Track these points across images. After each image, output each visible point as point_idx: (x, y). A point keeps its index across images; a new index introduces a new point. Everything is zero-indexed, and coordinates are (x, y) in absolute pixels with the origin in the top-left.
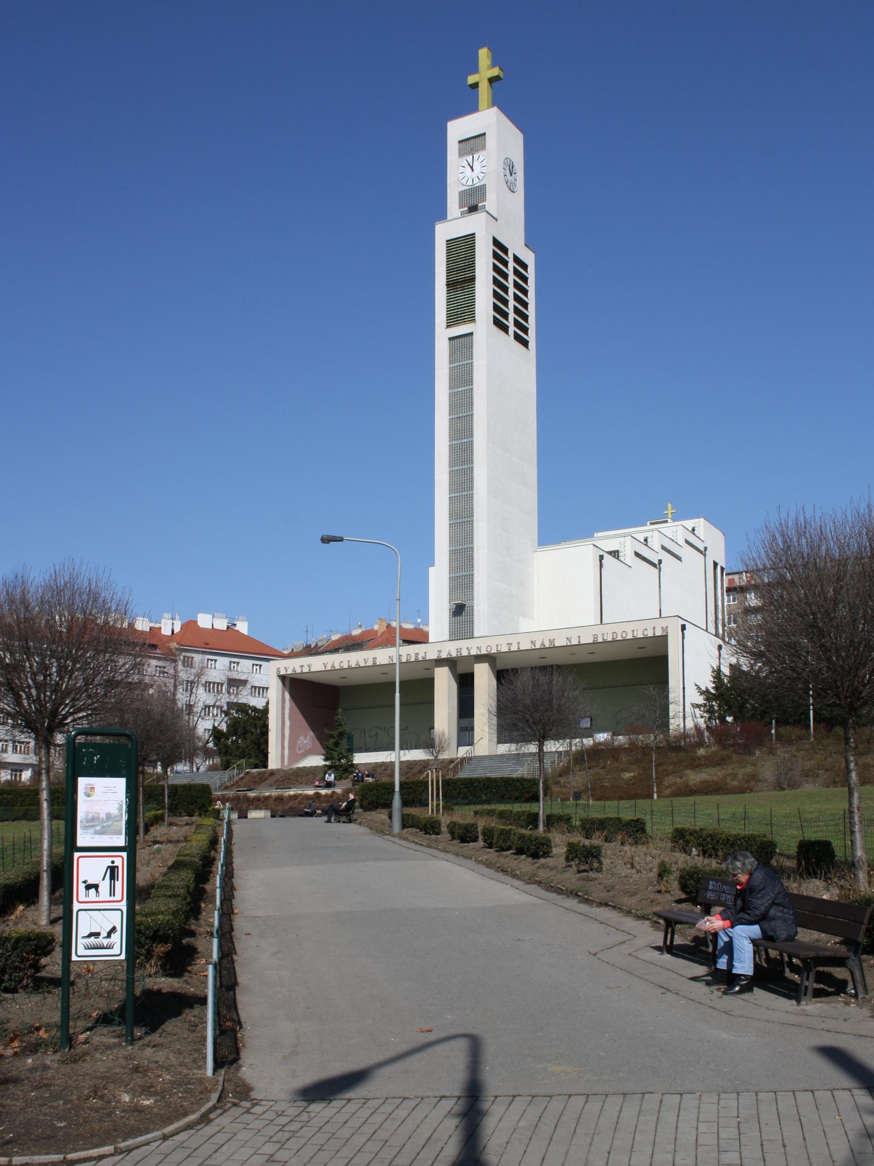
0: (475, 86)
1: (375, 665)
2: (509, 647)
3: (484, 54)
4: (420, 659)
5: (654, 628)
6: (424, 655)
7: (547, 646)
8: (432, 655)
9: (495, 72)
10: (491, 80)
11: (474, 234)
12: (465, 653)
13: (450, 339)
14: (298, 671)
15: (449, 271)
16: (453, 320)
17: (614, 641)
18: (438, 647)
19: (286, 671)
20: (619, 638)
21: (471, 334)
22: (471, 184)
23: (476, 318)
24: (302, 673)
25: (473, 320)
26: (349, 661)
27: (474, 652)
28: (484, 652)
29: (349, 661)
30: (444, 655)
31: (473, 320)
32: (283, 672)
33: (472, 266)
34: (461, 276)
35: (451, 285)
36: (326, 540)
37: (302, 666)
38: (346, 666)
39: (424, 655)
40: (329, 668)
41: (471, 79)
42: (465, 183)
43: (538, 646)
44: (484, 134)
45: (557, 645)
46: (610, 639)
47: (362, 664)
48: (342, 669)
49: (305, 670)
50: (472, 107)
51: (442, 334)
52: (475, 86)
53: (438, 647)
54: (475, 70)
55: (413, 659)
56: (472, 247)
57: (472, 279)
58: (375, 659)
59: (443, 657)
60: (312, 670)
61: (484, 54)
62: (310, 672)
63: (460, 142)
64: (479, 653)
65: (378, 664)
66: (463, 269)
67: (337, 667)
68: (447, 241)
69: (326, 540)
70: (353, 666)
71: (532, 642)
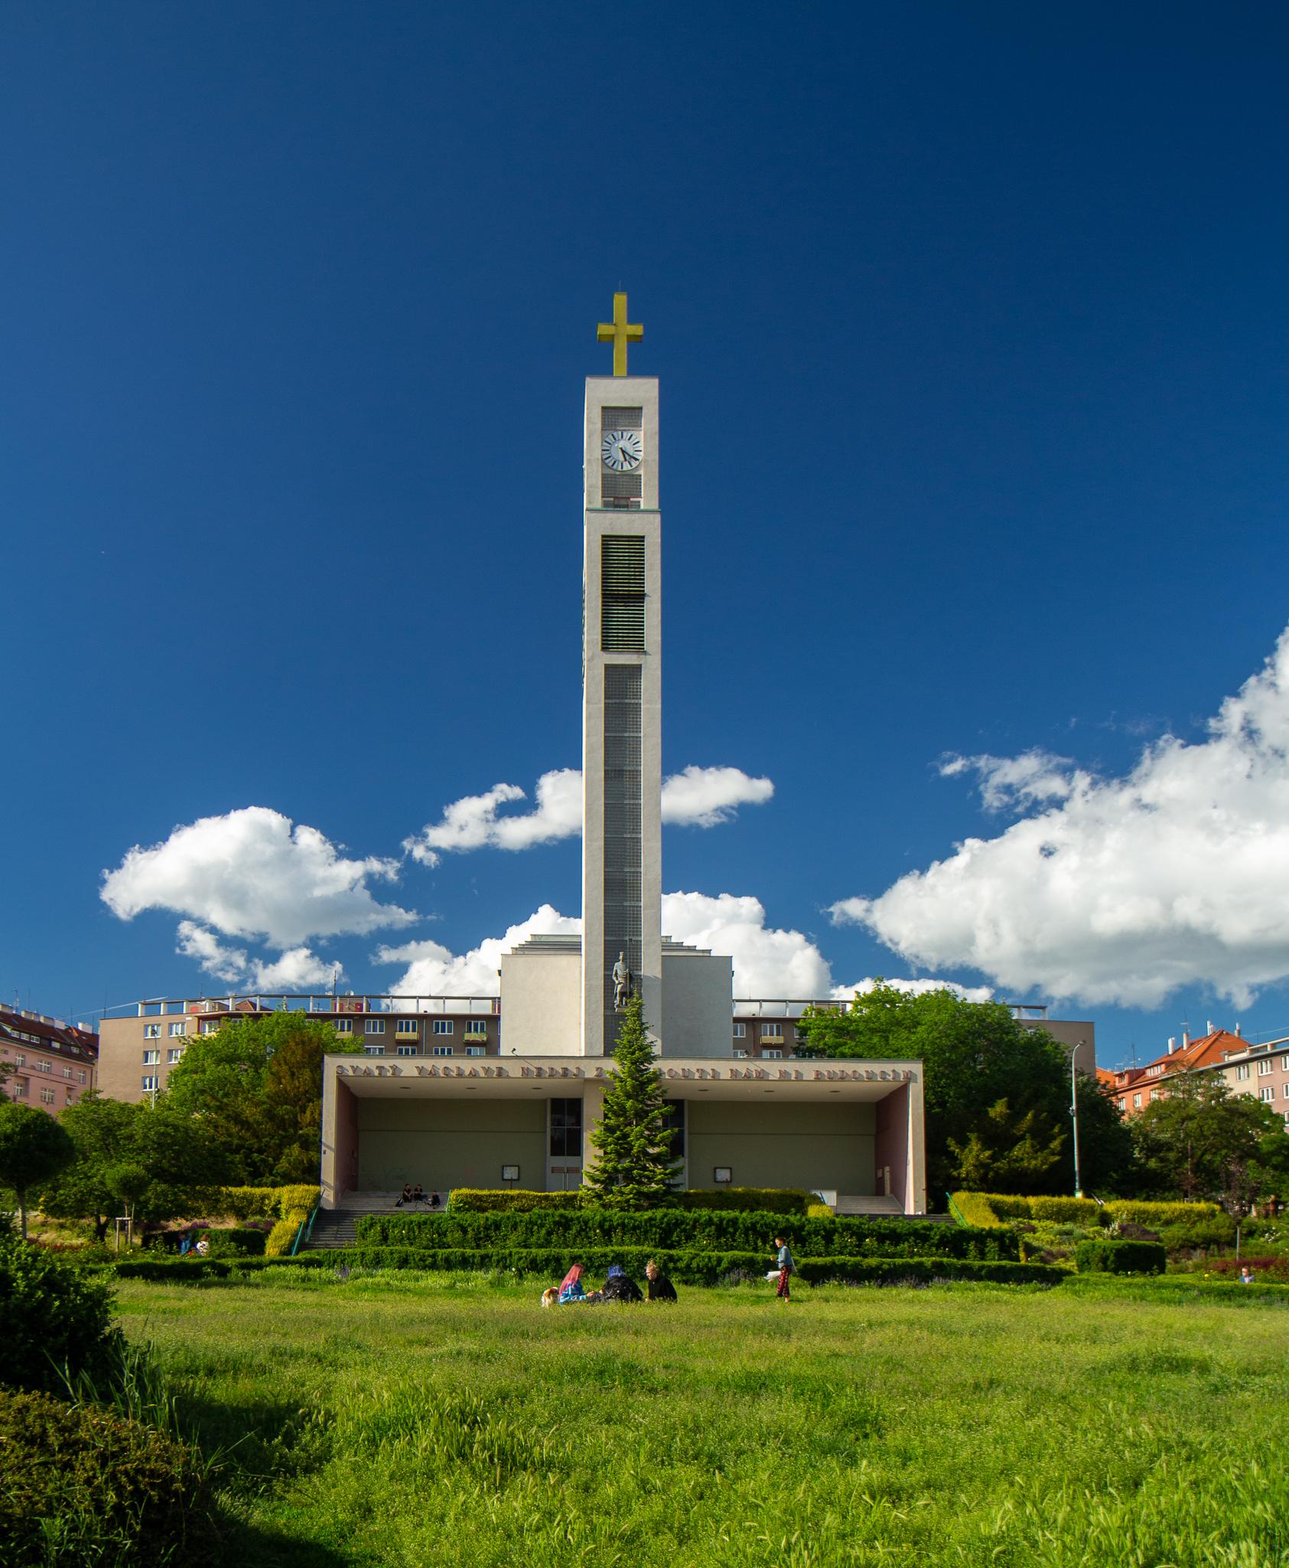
3: (620, 301)
9: (638, 330)
10: (632, 340)
25: (640, 650)
31: (640, 650)
34: (623, 589)
41: (603, 329)
44: (641, 408)
51: (594, 661)
54: (609, 319)
57: (640, 597)
61: (620, 301)
68: (603, 536)
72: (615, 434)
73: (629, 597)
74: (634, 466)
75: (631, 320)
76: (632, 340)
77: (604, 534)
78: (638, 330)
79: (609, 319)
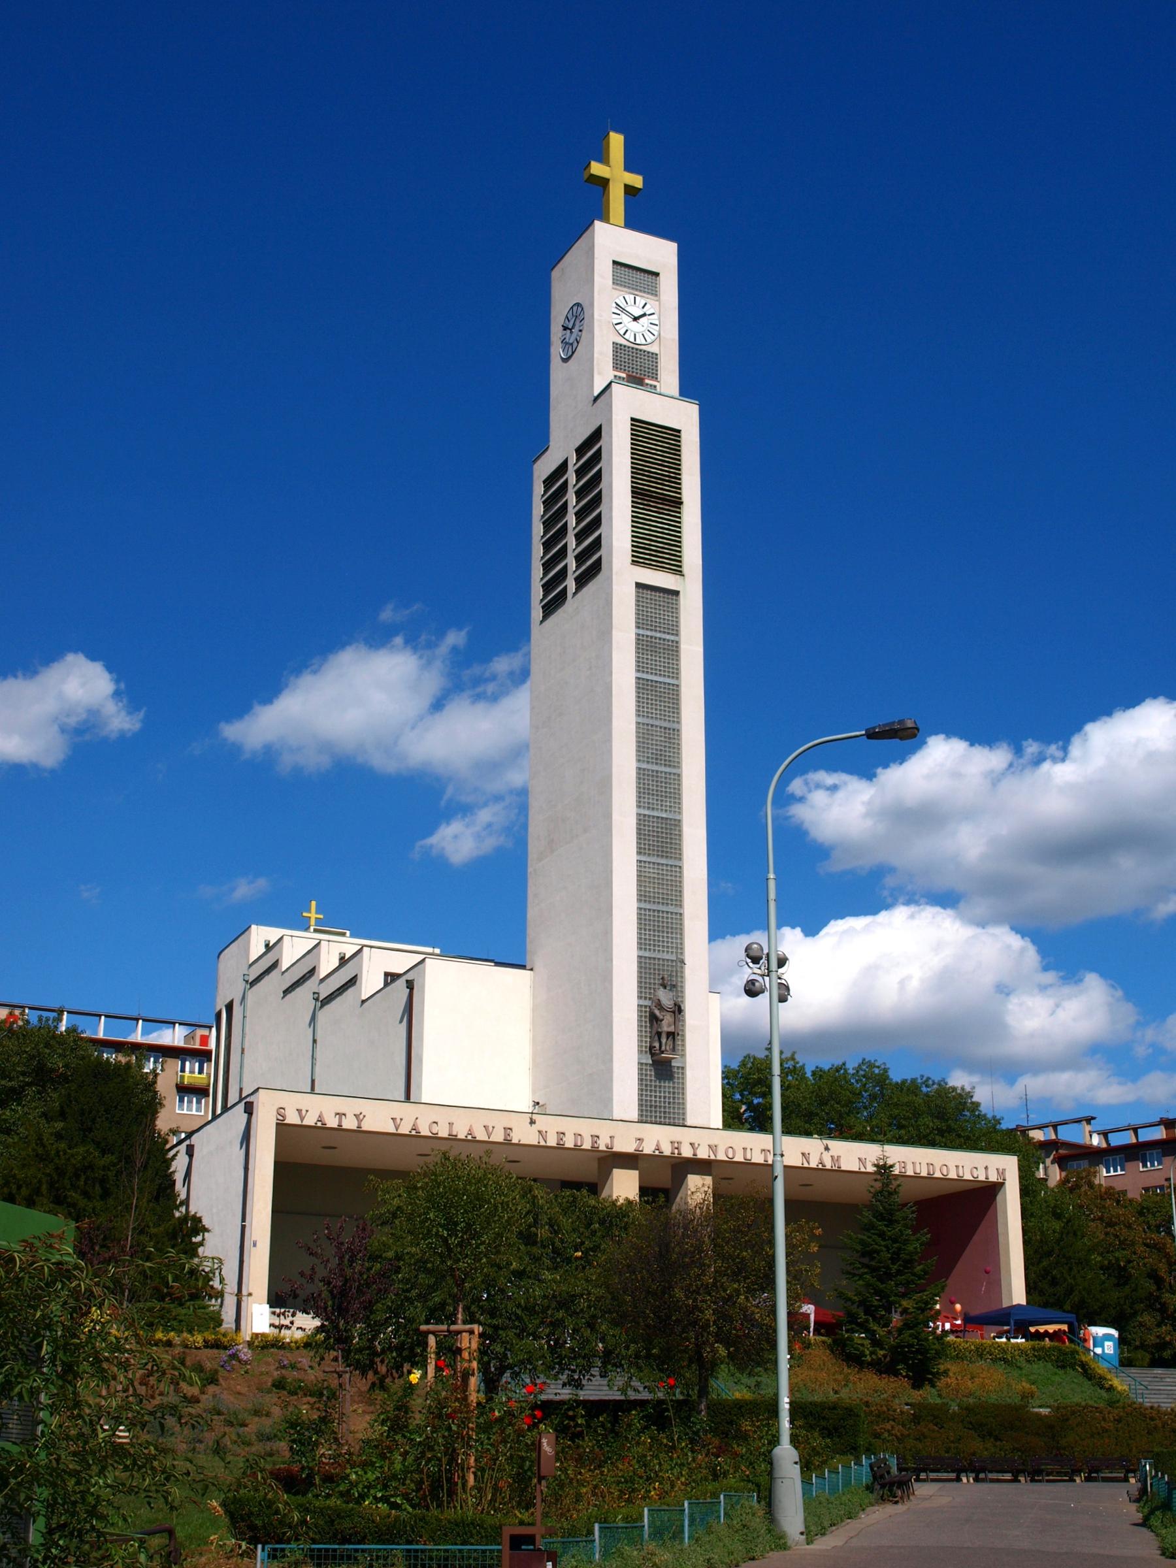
0: (604, 183)
1: (508, 1143)
2: (766, 1156)
3: (616, 141)
4: (602, 1148)
5: (986, 1168)
7: (828, 1167)
9: (637, 181)
10: (629, 190)
11: (679, 431)
12: (687, 1152)
13: (639, 586)
14: (332, 1122)
15: (636, 472)
16: (643, 555)
17: (930, 1178)
19: (302, 1119)
20: (938, 1175)
21: (677, 593)
22: (632, 340)
24: (339, 1129)
25: (678, 571)
26: (451, 1124)
27: (703, 1154)
28: (721, 1156)
29: (451, 1124)
30: (648, 1149)
31: (678, 571)
32: (292, 1118)
33: (675, 479)
35: (636, 492)
37: (341, 1115)
38: (444, 1133)
39: (608, 1141)
40: (405, 1129)
41: (597, 168)
42: (622, 333)
43: (813, 1164)
44: (657, 274)
45: (843, 1168)
46: (924, 1174)
47: (481, 1136)
48: (435, 1138)
49: (350, 1123)
50: (605, 218)
52: (604, 183)
54: (604, 159)
55: (587, 1145)
56: (676, 451)
57: (678, 503)
58: (508, 1130)
59: (646, 1151)
60: (366, 1126)
61: (616, 141)
62: (359, 1132)
63: (615, 262)
64: (713, 1157)
65: (515, 1141)
66: (660, 479)
67: (425, 1132)
68: (632, 419)
70: (461, 1136)
71: (803, 1154)
72: (627, 297)
73: (665, 500)
74: (649, 341)
75: (628, 167)
76: (629, 190)
78: (637, 181)
79: (604, 159)
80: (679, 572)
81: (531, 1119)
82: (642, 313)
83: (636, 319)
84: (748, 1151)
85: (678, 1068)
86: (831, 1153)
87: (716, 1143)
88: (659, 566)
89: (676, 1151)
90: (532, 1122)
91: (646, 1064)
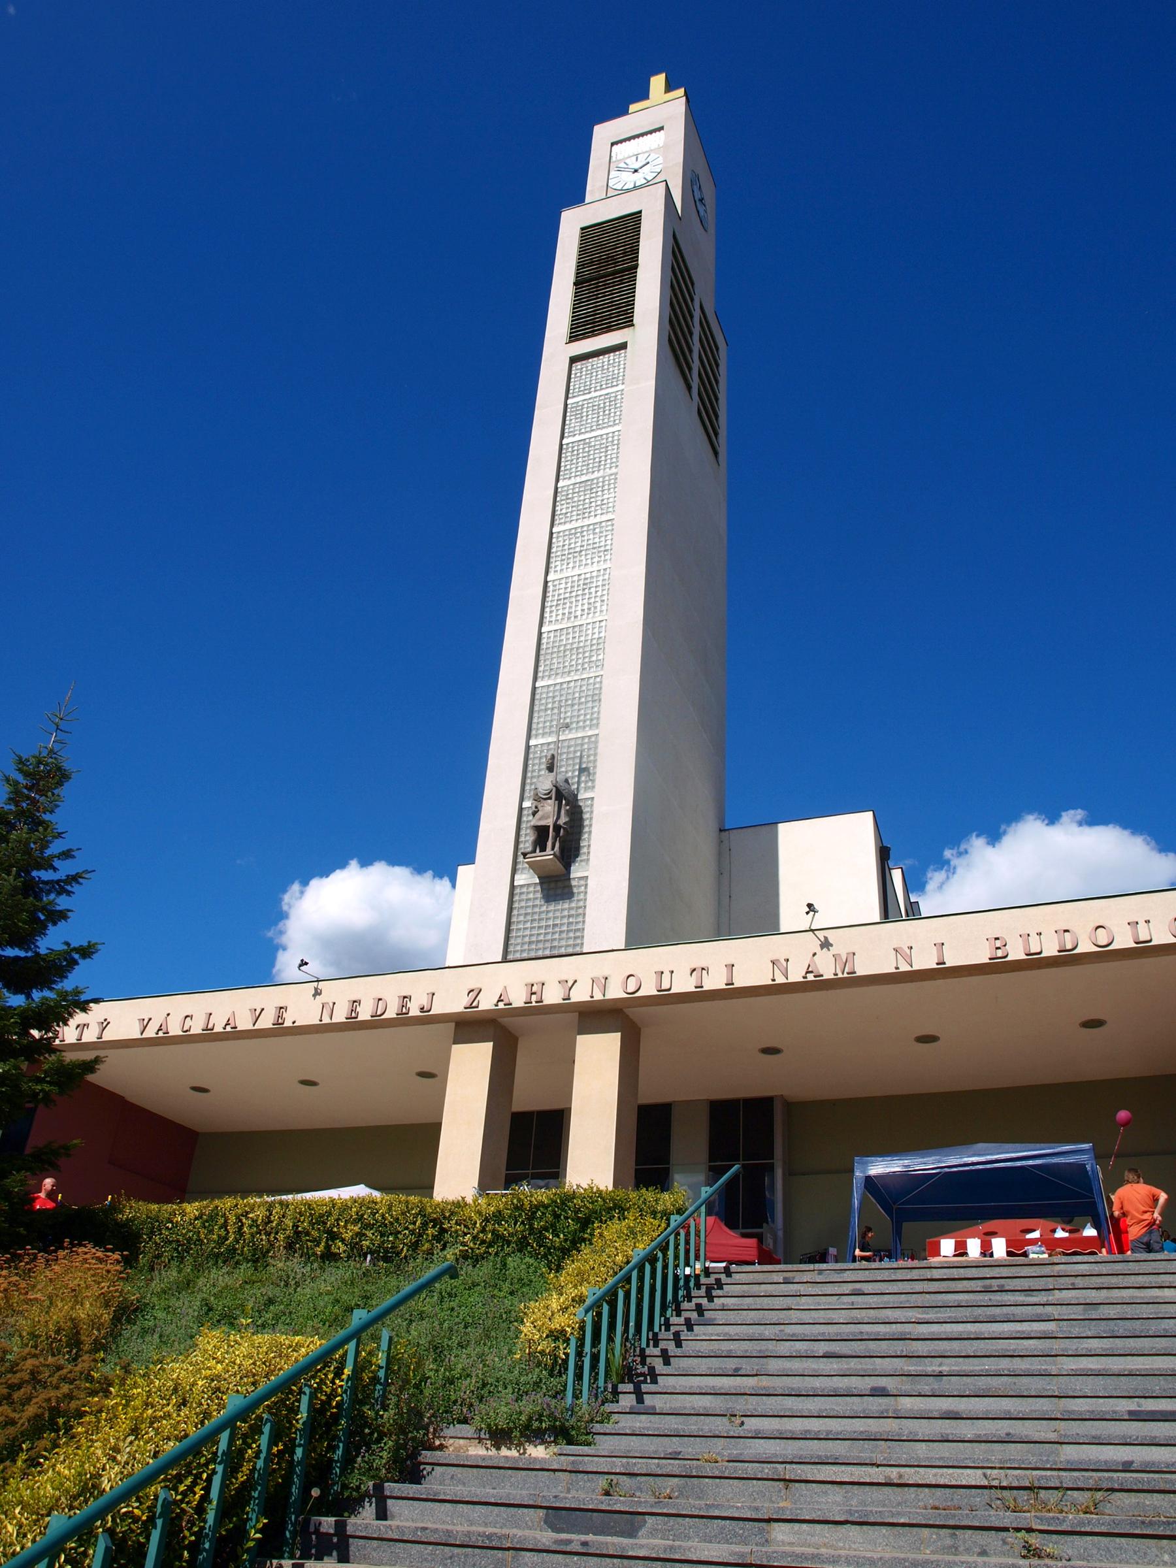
4: (414, 1012)
6: (425, 1002)
7: (828, 975)
8: (451, 1003)
12: (553, 996)
13: (574, 360)
18: (471, 979)
21: (623, 346)
23: (634, 322)
25: (630, 323)
27: (580, 995)
28: (615, 992)
30: (486, 1003)
31: (630, 323)
36: (312, 1083)
45: (860, 972)
53: (471, 979)
55: (391, 1014)
64: (598, 996)
65: (288, 1023)
68: (582, 229)
69: (312, 1083)
77: (583, 226)
80: (633, 325)
81: (316, 989)
82: (644, 163)
83: (636, 171)
84: (666, 976)
85: (580, 878)
86: (833, 950)
87: (606, 974)
88: (609, 329)
89: (534, 998)
90: (317, 993)
91: (529, 885)
